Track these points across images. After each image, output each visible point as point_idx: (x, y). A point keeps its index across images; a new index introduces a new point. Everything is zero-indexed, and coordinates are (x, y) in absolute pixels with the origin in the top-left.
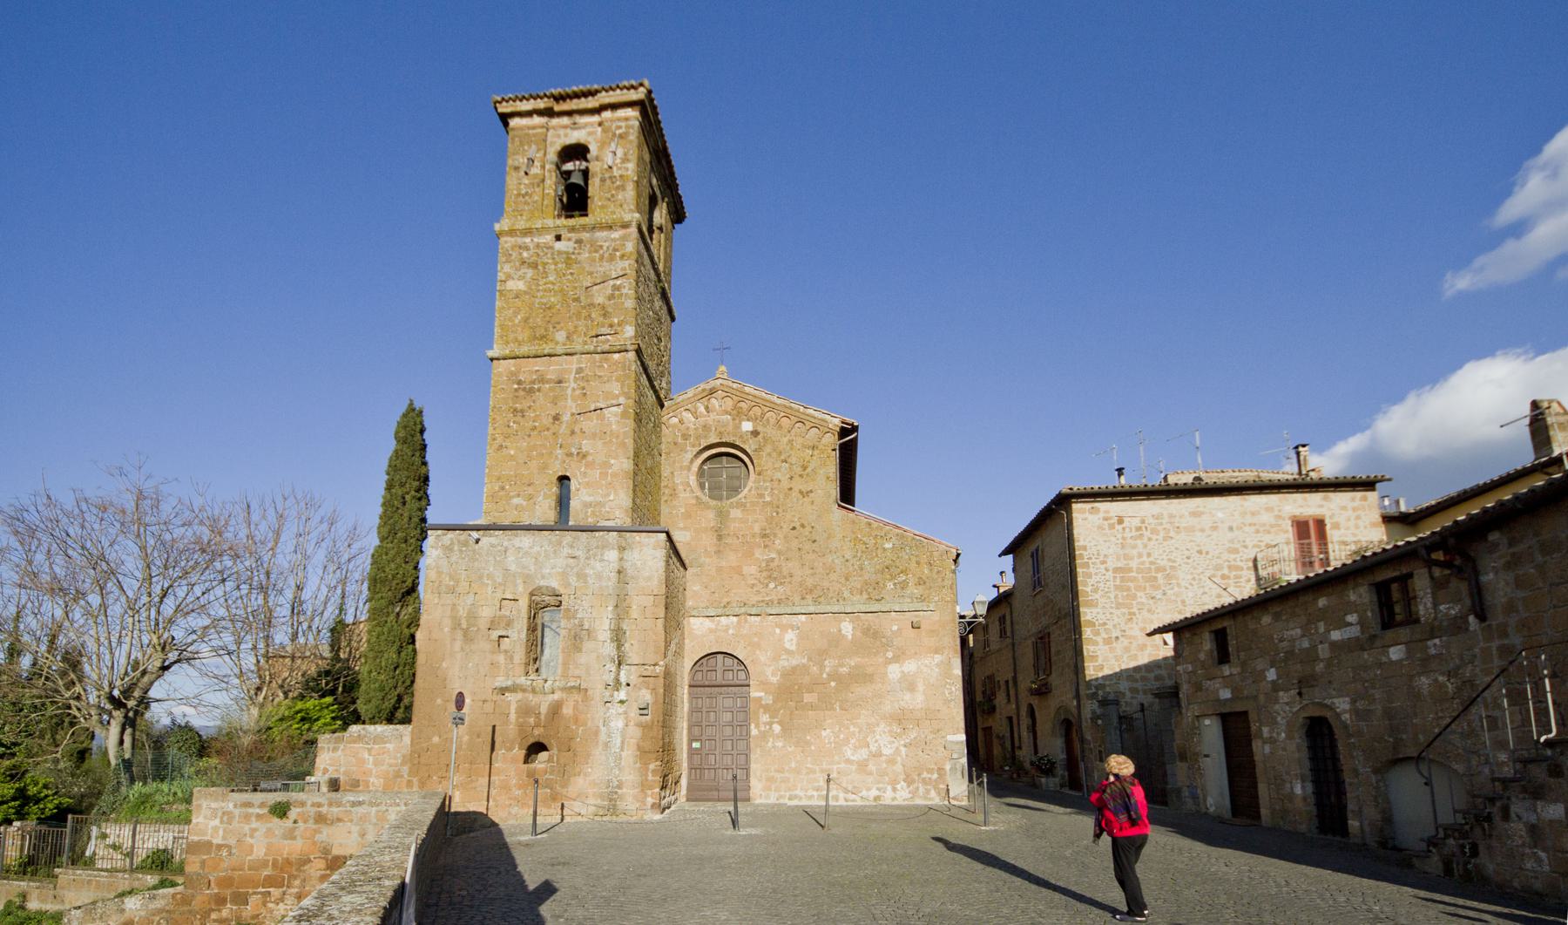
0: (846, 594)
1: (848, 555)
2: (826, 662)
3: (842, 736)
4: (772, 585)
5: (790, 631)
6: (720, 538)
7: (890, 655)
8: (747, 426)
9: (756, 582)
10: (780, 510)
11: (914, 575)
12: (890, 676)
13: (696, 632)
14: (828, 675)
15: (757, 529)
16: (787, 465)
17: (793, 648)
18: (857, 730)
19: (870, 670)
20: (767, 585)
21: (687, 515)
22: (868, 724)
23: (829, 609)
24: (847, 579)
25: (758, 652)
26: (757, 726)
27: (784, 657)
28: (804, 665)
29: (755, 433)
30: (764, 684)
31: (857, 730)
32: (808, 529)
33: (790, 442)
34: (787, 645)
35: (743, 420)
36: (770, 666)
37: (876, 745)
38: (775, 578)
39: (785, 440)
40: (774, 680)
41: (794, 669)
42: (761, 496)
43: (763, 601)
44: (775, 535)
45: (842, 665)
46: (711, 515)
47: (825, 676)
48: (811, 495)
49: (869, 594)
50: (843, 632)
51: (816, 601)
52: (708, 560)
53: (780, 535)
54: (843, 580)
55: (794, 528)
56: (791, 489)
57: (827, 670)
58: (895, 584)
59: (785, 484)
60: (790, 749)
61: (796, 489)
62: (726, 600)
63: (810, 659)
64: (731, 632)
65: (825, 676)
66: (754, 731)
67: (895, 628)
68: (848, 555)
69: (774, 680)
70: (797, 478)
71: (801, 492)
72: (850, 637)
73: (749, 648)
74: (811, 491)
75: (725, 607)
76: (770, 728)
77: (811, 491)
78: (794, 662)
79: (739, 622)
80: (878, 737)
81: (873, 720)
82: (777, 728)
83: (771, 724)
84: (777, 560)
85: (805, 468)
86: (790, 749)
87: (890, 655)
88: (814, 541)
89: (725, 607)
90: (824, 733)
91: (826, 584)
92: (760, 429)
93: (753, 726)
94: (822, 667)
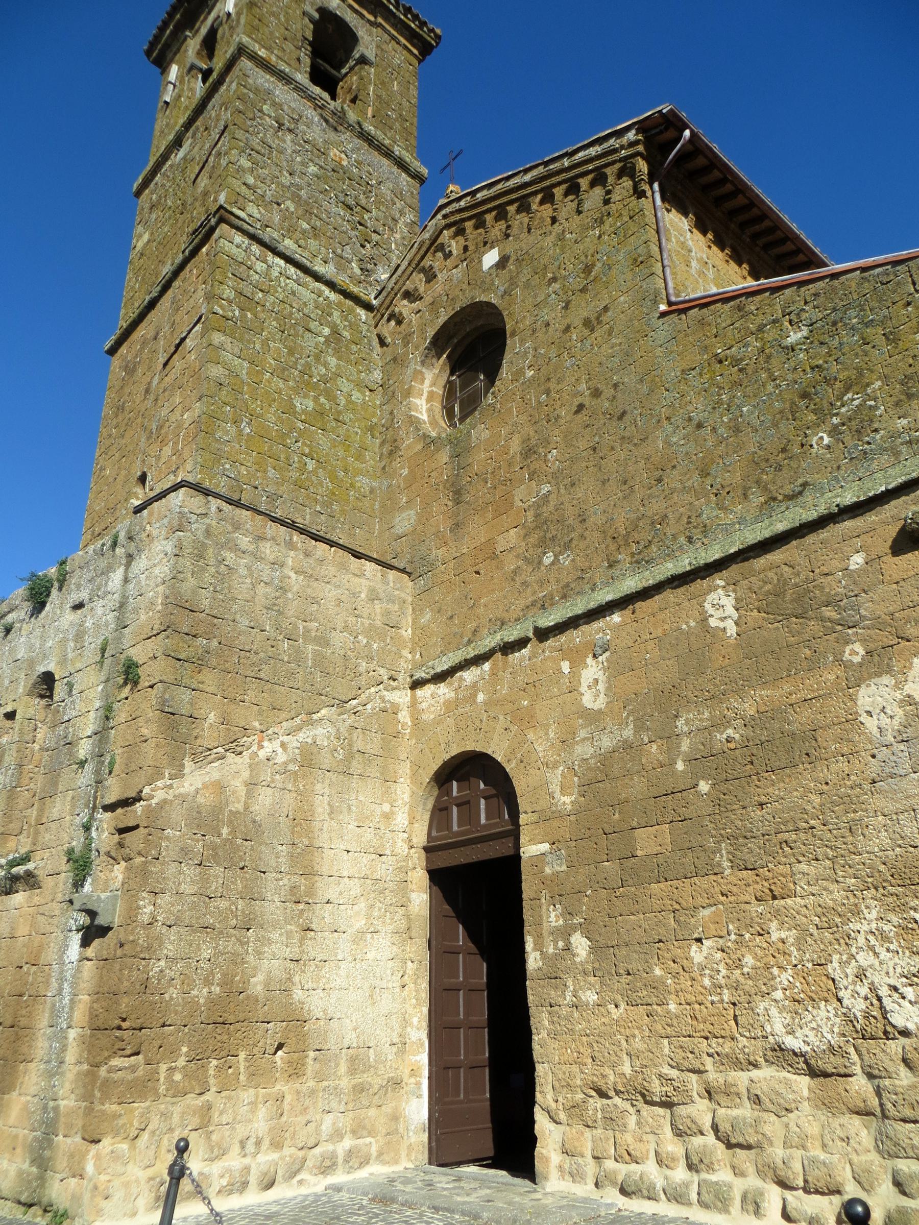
0: (709, 513)
1: (698, 408)
2: (680, 723)
3: (749, 960)
4: (548, 559)
5: (589, 660)
6: (458, 495)
7: (855, 652)
8: (491, 258)
9: (520, 563)
10: (552, 385)
11: (885, 378)
12: (871, 724)
13: (424, 717)
14: (688, 761)
15: (515, 446)
16: (556, 286)
17: (600, 703)
18: (791, 935)
19: (802, 718)
20: (540, 562)
21: (411, 481)
22: (824, 911)
23: (670, 568)
24: (704, 474)
25: (531, 736)
26: (538, 947)
27: (583, 734)
28: (627, 746)
29: (502, 263)
30: (547, 817)
31: (791, 935)
32: (608, 392)
33: (561, 238)
34: (588, 700)
35: (484, 253)
36: (555, 765)
37: (864, 990)
38: (553, 539)
39: (550, 239)
40: (566, 801)
41: (606, 759)
42: (520, 372)
43: (533, 604)
44: (546, 441)
45: (725, 723)
46: (444, 456)
47: (680, 766)
48: (604, 319)
49: (766, 489)
50: (713, 622)
51: (640, 562)
52: (440, 552)
53: (556, 437)
54: (695, 480)
55: (581, 407)
56: (567, 329)
57: (685, 745)
58: (834, 432)
59: (557, 326)
60: (616, 1013)
61: (577, 322)
62: (470, 627)
63: (640, 727)
64: (481, 697)
65: (680, 766)
66: (533, 961)
67: (857, 560)
68: (698, 408)
69: (566, 801)
70: (575, 300)
71: (587, 323)
72: (732, 630)
73: (514, 728)
74: (606, 309)
75: (470, 642)
76: (568, 948)
77: (606, 309)
78: (607, 742)
79: (493, 673)
80: (865, 959)
81: (839, 895)
82: (580, 944)
83: (565, 933)
84: (553, 497)
85: (588, 269)
86: (616, 1013)
87: (855, 652)
88: (621, 417)
89: (470, 642)
90: (697, 954)
91: (656, 507)
92: (509, 250)
93: (529, 945)
94: (670, 738)
